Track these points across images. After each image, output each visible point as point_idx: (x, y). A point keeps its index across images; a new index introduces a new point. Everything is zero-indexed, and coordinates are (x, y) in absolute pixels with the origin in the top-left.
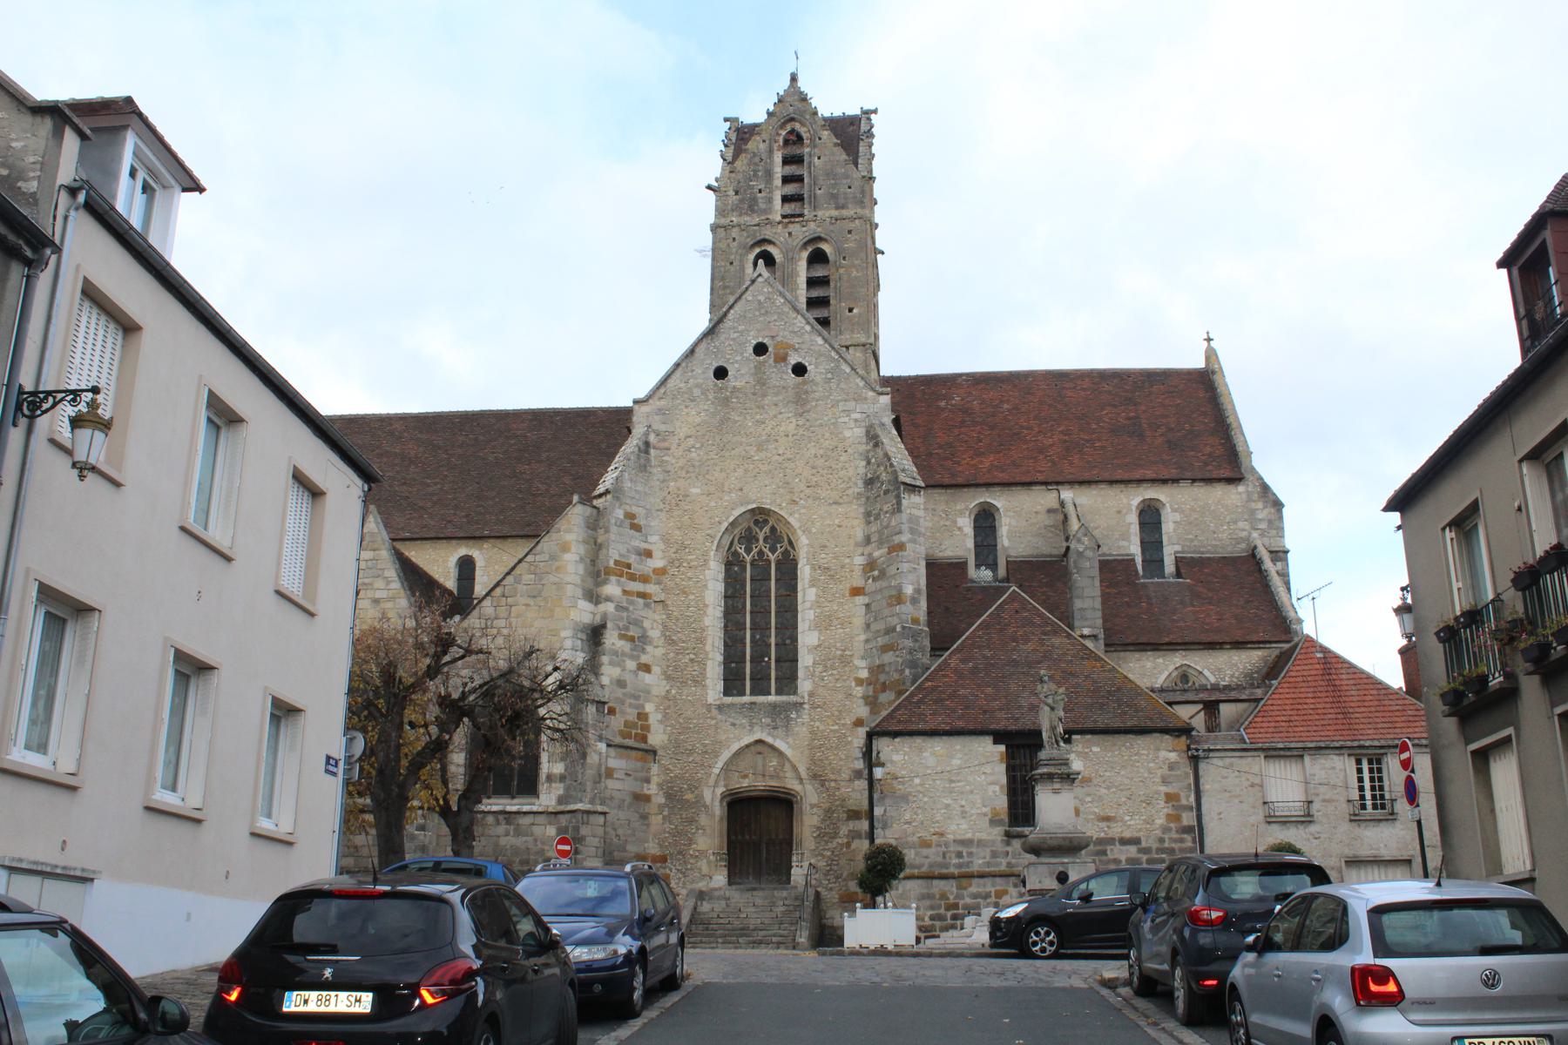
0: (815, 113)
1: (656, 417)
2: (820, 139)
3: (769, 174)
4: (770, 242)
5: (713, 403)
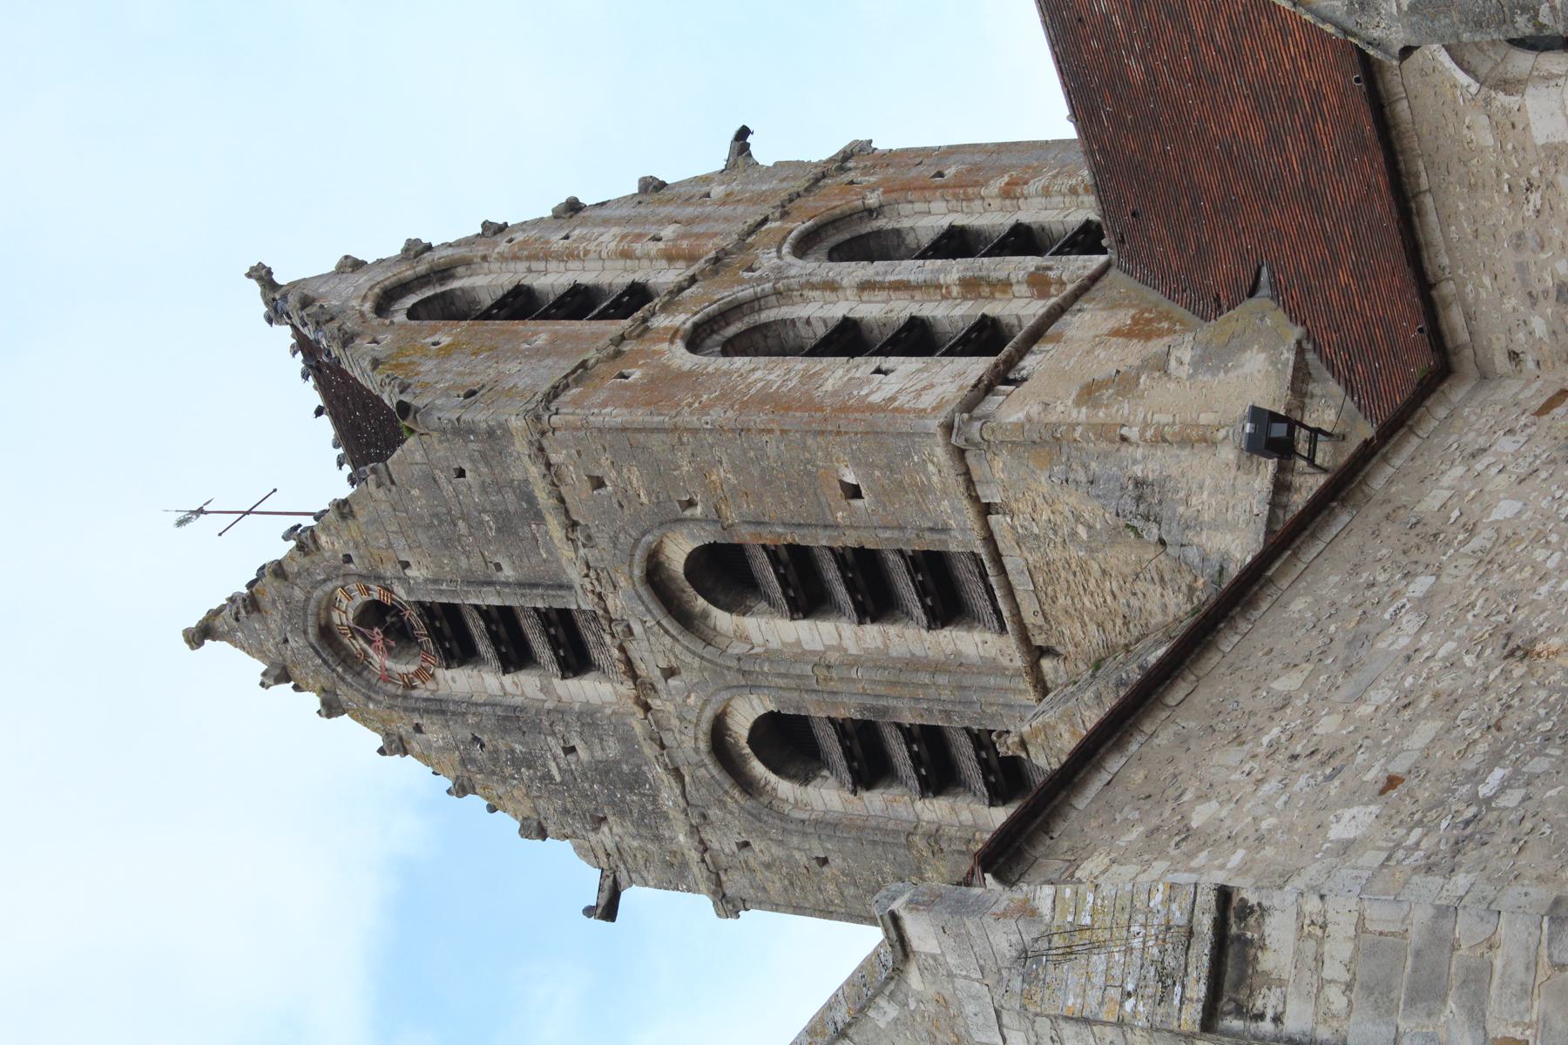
0: (277, 570)
2: (348, 559)
3: (512, 718)
4: (719, 733)
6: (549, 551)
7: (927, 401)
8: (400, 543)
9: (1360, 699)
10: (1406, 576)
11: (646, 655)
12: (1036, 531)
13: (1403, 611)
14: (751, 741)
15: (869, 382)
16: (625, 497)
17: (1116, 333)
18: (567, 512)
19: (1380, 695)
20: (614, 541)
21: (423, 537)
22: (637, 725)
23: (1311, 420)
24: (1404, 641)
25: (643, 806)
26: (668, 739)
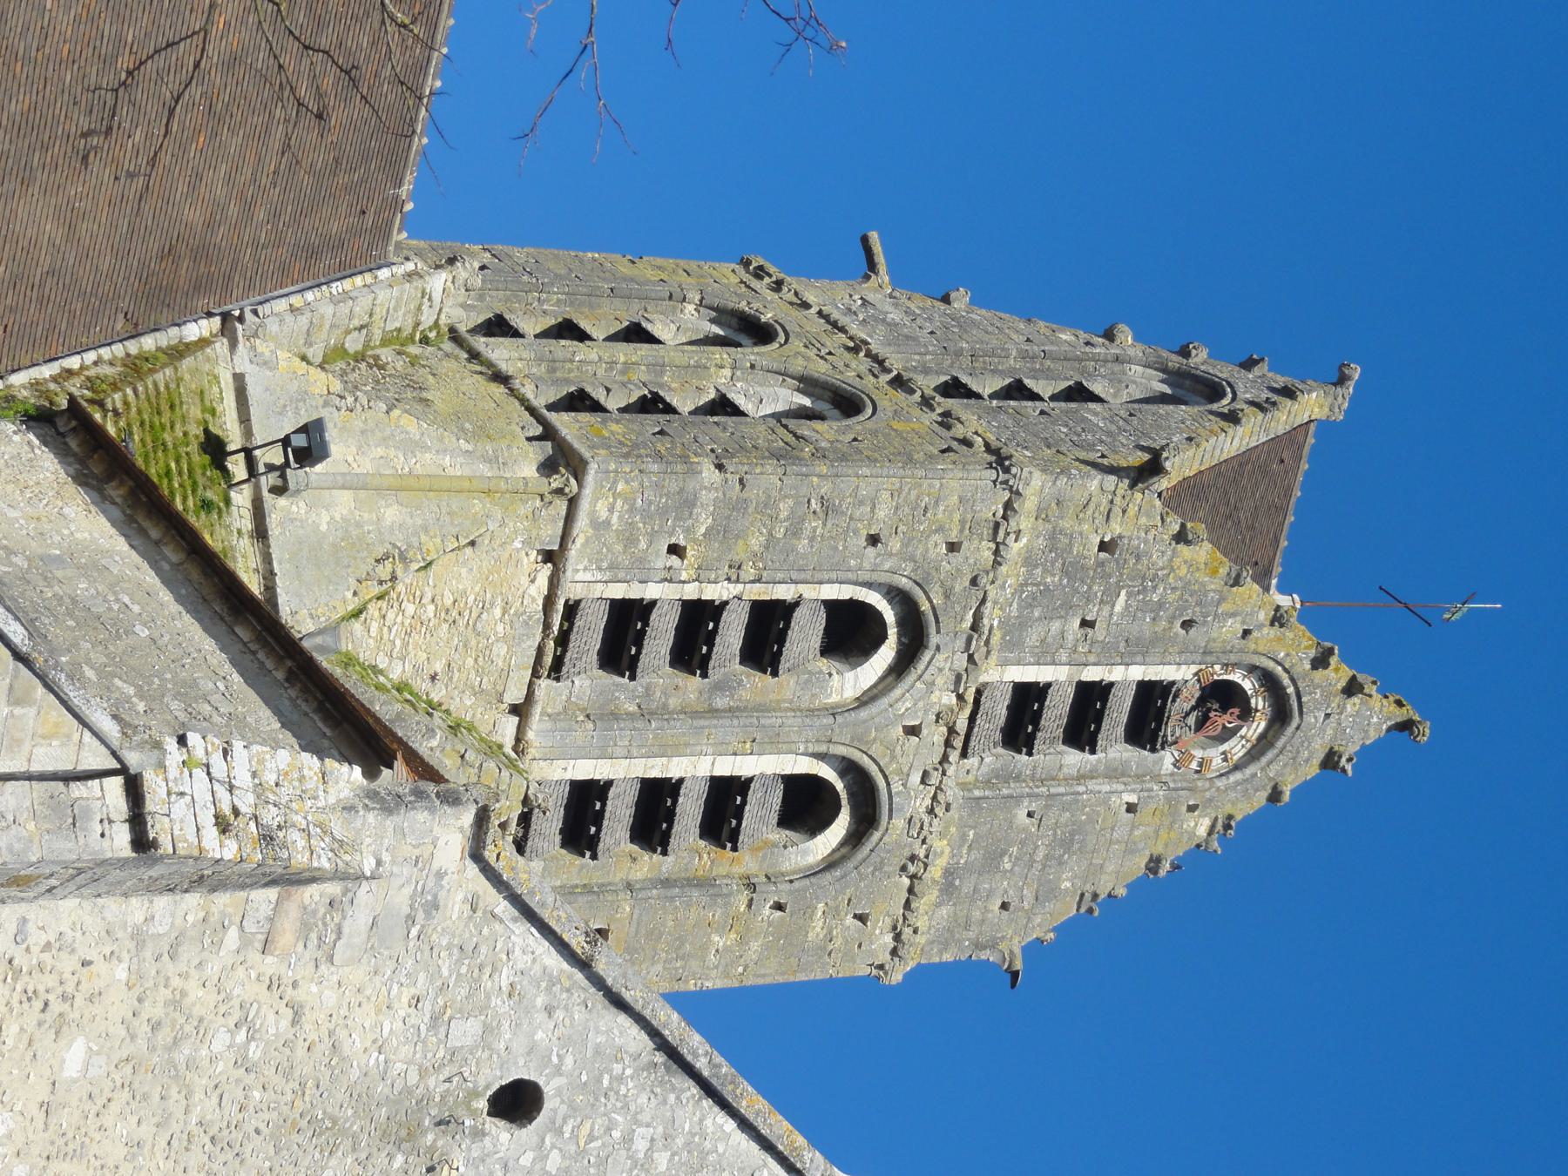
1: (408, 891)
2: (1192, 809)
3: (1135, 650)
5: (407, 1090)
6: (964, 837)
14: (882, 638)
16: (833, 912)
25: (1045, 571)
26: (961, 661)
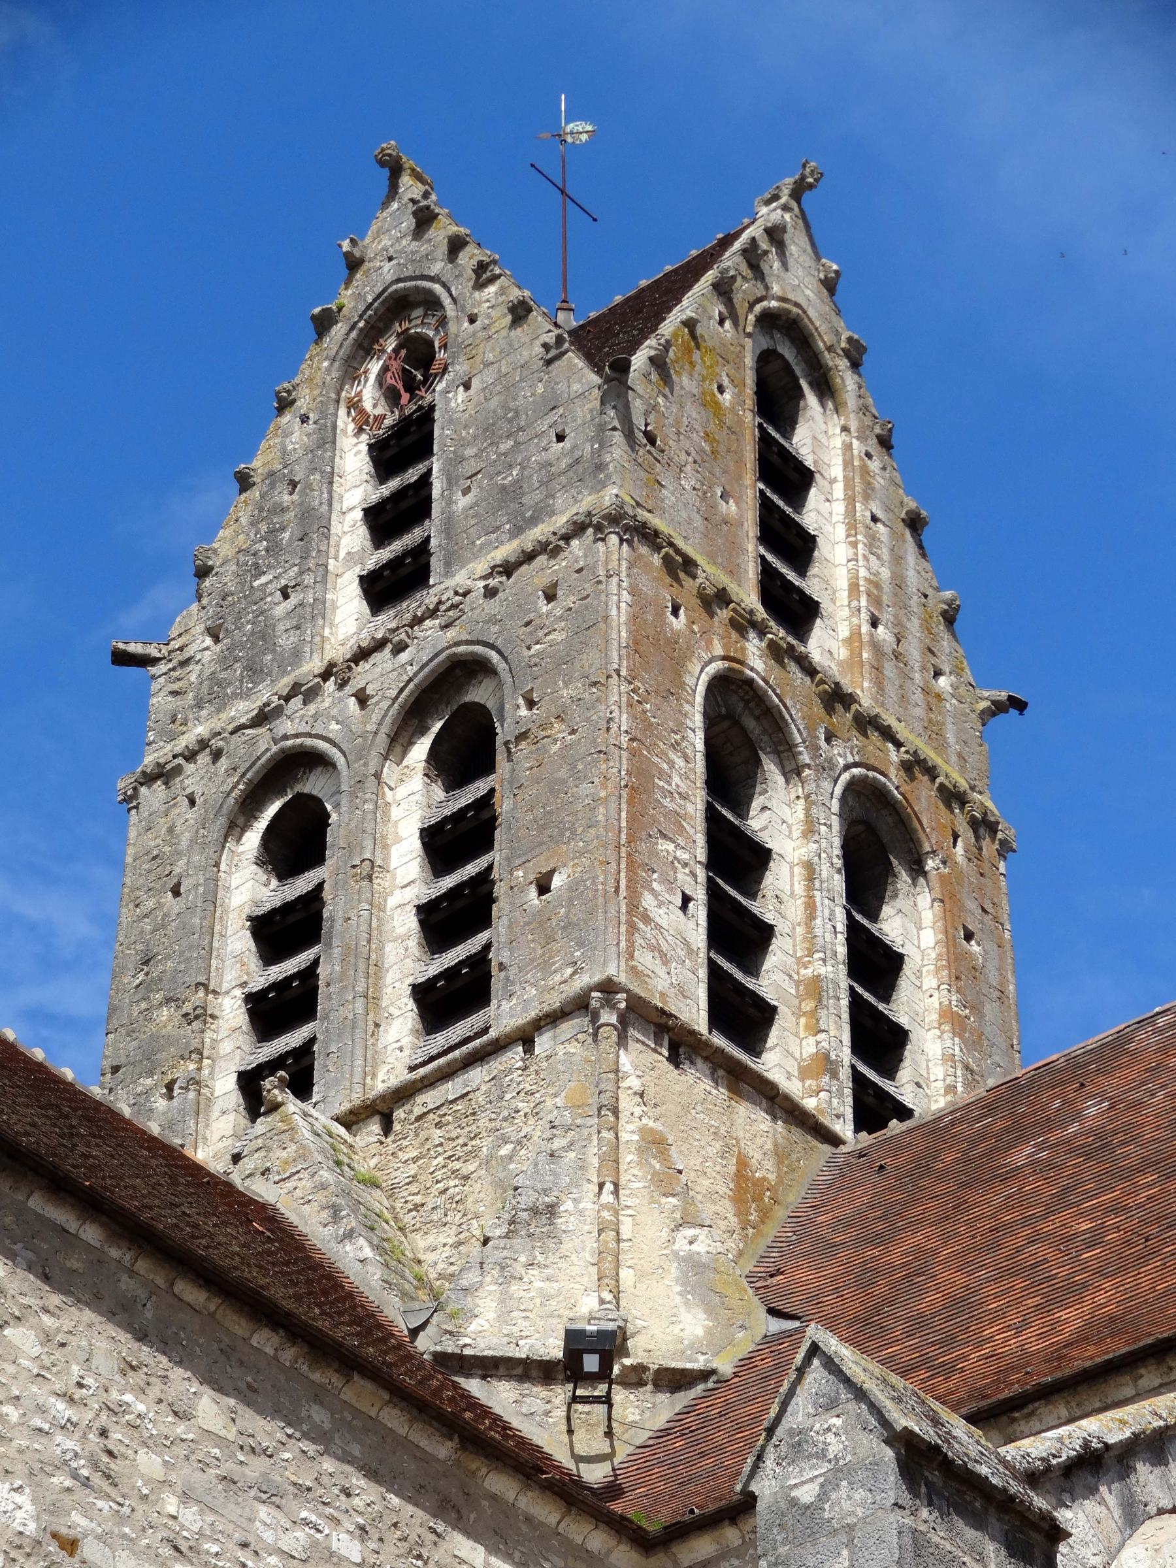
6: (483, 546)
7: (645, 959)
8: (489, 376)
9: (186, 1497)
10: (362, 1528)
11: (378, 670)
12: (508, 1096)
13: (312, 1532)
14: (299, 796)
15: (671, 891)
17: (743, 1162)
18: (519, 564)
19: (191, 1518)
20: (494, 620)
21: (494, 403)
22: (316, 665)
23: (620, 1395)
24: (268, 1536)
